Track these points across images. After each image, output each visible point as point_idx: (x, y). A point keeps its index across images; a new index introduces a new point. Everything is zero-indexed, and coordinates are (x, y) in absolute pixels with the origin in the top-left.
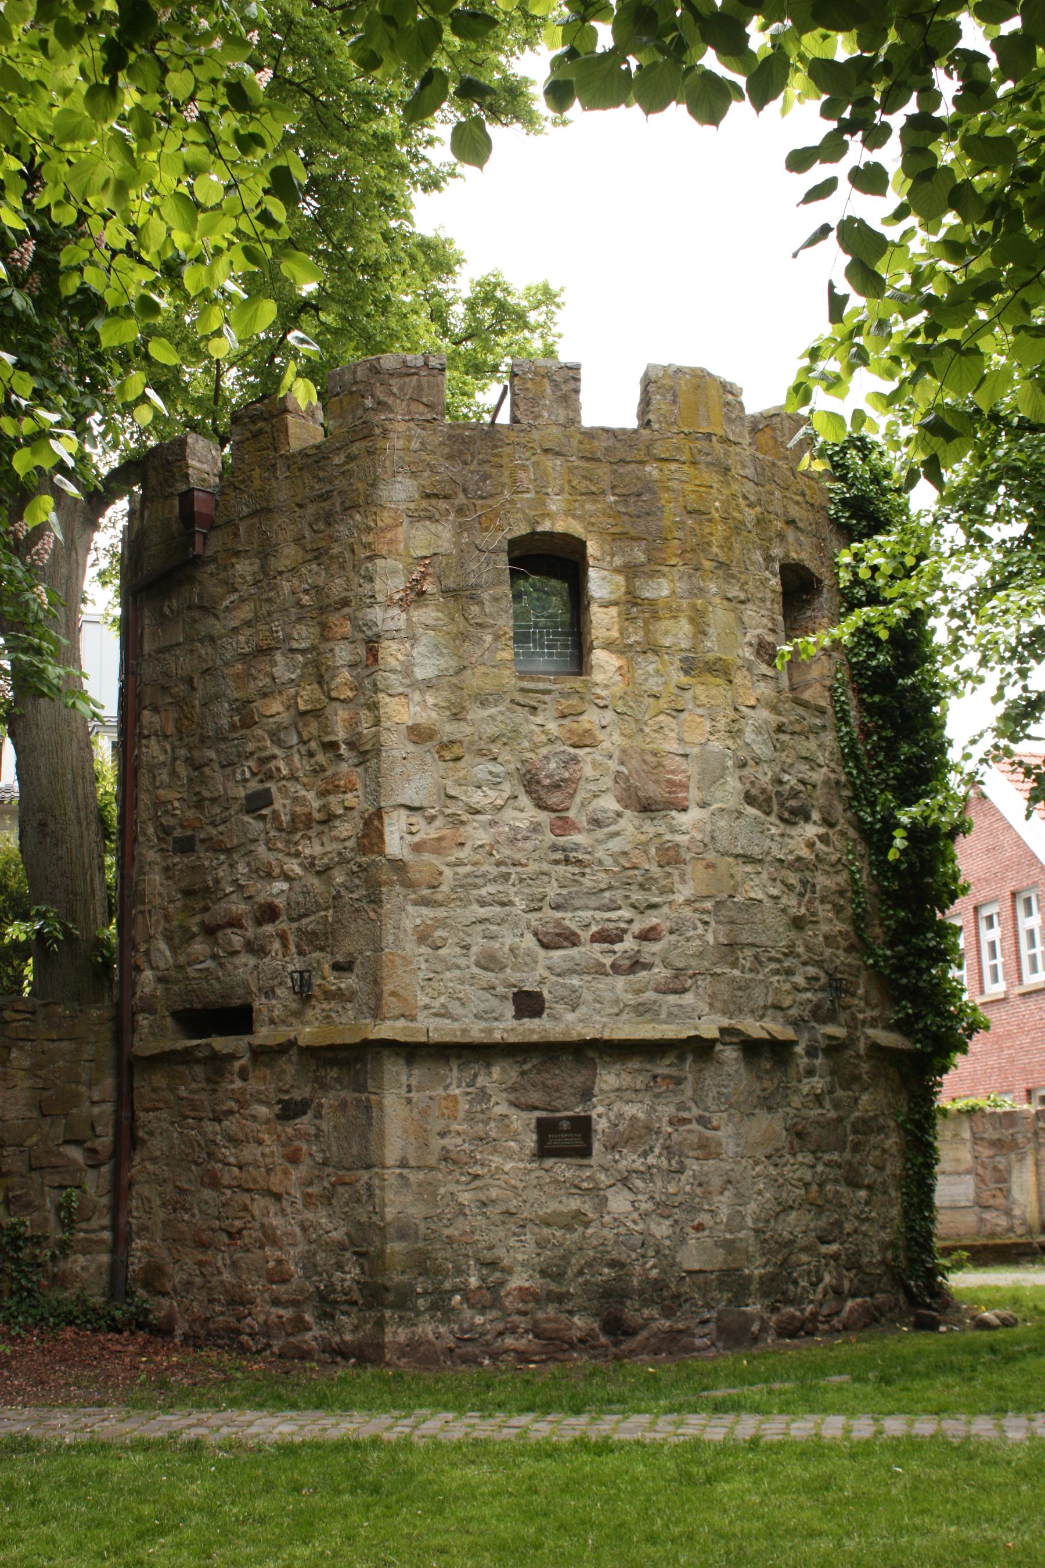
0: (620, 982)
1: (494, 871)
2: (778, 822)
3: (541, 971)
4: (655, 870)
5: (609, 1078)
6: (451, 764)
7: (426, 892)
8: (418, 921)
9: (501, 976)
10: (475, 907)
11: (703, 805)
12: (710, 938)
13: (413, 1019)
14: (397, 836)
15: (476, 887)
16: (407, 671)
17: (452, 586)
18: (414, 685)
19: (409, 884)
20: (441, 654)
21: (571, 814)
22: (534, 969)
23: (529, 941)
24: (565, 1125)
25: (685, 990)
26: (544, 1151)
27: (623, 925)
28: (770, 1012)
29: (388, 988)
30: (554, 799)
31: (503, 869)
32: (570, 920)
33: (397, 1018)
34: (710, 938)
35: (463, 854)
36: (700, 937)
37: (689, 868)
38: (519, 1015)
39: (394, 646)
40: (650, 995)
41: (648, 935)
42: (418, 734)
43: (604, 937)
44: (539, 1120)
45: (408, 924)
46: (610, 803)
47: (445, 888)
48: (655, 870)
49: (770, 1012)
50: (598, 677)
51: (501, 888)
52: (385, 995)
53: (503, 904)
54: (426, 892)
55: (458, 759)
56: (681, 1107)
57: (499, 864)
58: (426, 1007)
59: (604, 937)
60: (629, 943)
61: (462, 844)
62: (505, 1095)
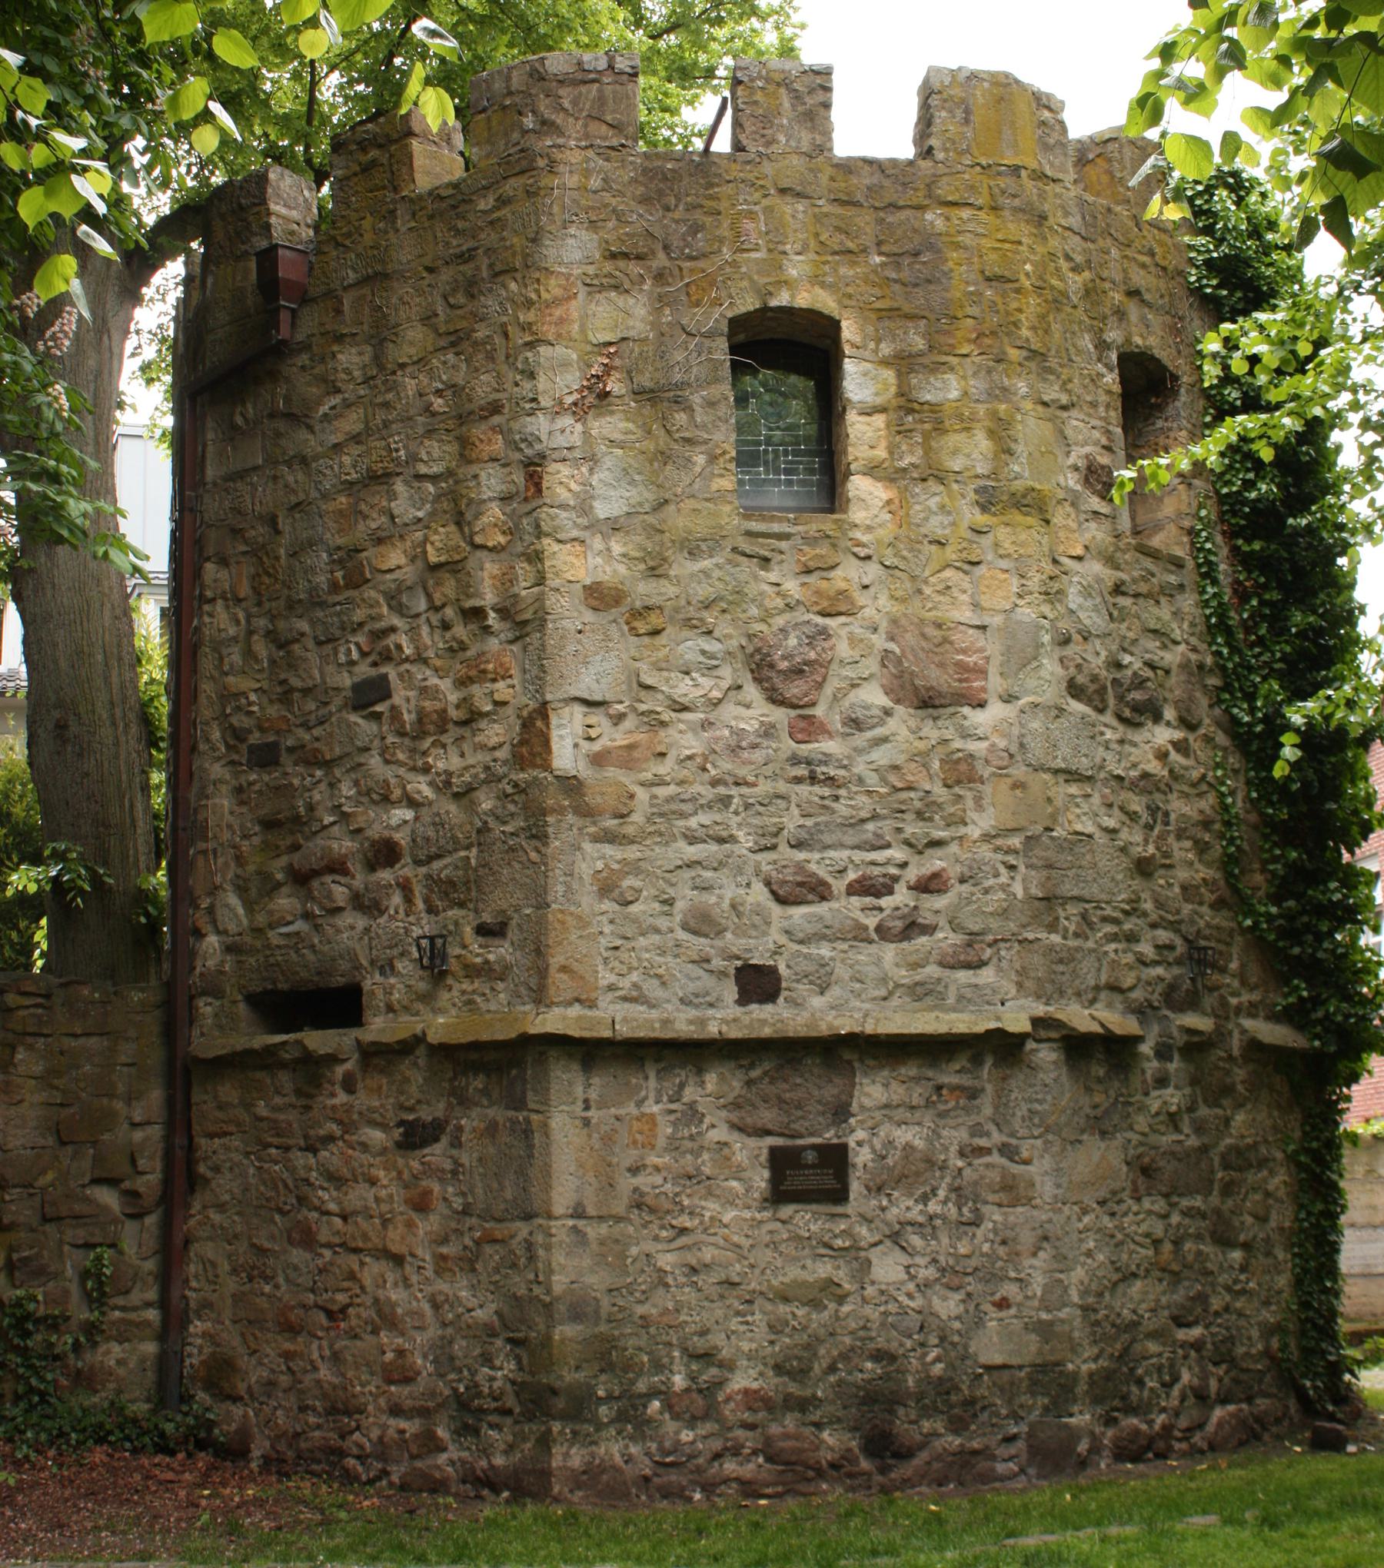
0: (889, 952)
1: (708, 793)
2: (1115, 723)
3: (776, 936)
4: (939, 792)
5: (873, 1090)
6: (646, 640)
7: (611, 823)
8: (600, 865)
9: (718, 943)
10: (681, 844)
11: (1008, 698)
12: (1018, 889)
13: (592, 1004)
15: (683, 815)
16: (584, 507)
17: (648, 384)
18: (593, 526)
19: (587, 812)
20: (632, 482)
21: (819, 711)
22: (765, 934)
23: (759, 894)
24: (810, 1157)
25: (982, 964)
26: (779, 1195)
27: (893, 871)
29: (556, 960)
30: (794, 689)
31: (722, 790)
32: (818, 864)
34: (1018, 889)
35: (664, 768)
36: (1004, 888)
37: (987, 789)
38: (744, 999)
39: (565, 470)
40: (932, 970)
41: (929, 885)
42: (599, 597)
43: (869, 888)
44: (773, 1150)
45: (585, 869)
46: (874, 696)
47: (637, 818)
48: (939, 792)
49: (1103, 995)
50: (857, 515)
51: (718, 818)
52: (552, 970)
53: (721, 841)
54: (611, 823)
55: (656, 632)
56: (977, 1131)
57: (715, 783)
58: (611, 988)
59: (869, 888)
60: (901, 897)
61: (663, 755)
62: (724, 1114)
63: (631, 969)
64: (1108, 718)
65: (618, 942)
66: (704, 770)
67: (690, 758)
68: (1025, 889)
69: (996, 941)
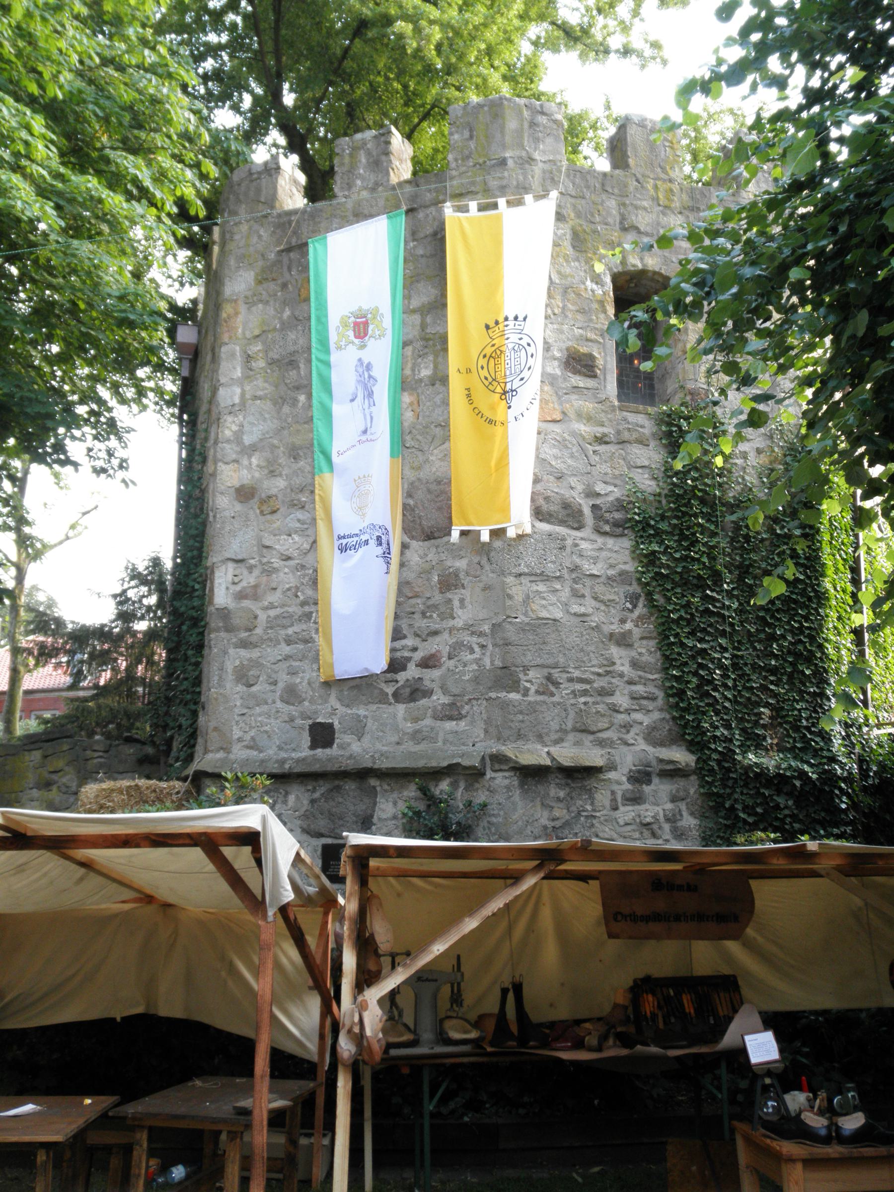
2: (595, 537)
4: (438, 598)
6: (269, 517)
7: (244, 635)
8: (237, 663)
9: (300, 708)
12: (487, 662)
13: (227, 750)
14: (224, 586)
15: (285, 627)
17: (276, 357)
19: (229, 629)
20: (265, 420)
22: (326, 701)
25: (460, 717)
27: (406, 654)
28: (571, 737)
31: (307, 609)
33: (218, 750)
34: (487, 662)
35: (274, 598)
36: (477, 661)
37: (466, 593)
39: (230, 419)
40: (428, 721)
41: (427, 663)
42: (245, 494)
45: (229, 666)
47: (259, 631)
48: (438, 598)
49: (571, 737)
51: (304, 627)
52: (210, 731)
53: (306, 641)
54: (244, 635)
55: (274, 512)
57: (303, 604)
58: (240, 740)
60: (412, 672)
62: (299, 822)
63: (251, 728)
64: (587, 532)
65: (245, 711)
66: (297, 596)
67: (289, 589)
68: (492, 662)
69: (470, 700)
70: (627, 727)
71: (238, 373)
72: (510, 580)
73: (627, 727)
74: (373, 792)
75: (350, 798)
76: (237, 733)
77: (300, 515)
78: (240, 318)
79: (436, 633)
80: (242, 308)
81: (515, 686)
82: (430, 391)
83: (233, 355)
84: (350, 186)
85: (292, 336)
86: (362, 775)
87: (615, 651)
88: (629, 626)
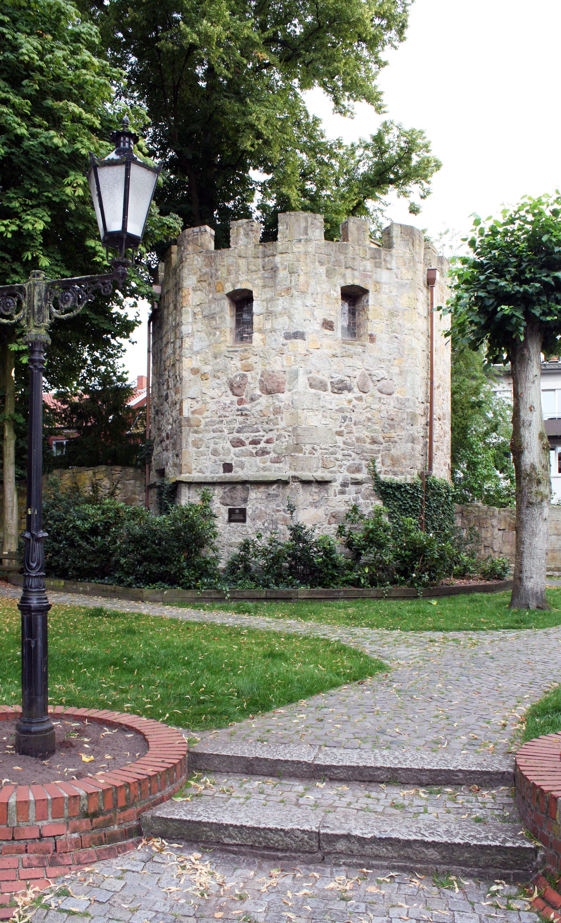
0: (258, 459)
1: (218, 419)
3: (232, 455)
4: (272, 417)
5: (254, 494)
11: (289, 391)
16: (191, 348)
18: (193, 353)
19: (190, 426)
21: (244, 397)
23: (229, 445)
24: (237, 511)
26: (230, 520)
30: (237, 391)
32: (242, 436)
37: (284, 415)
38: (225, 472)
39: (187, 339)
40: (269, 464)
42: (195, 371)
43: (255, 442)
44: (230, 509)
46: (258, 392)
47: (202, 427)
48: (272, 417)
50: (254, 343)
56: (278, 505)
59: (255, 442)
60: (262, 445)
70: (341, 466)
71: (190, 320)
72: (300, 411)
73: (341, 466)
74: (248, 490)
75: (239, 492)
76: (194, 466)
77: (218, 381)
78: (190, 296)
79: (271, 430)
80: (191, 292)
81: (301, 451)
82: (270, 334)
83: (188, 312)
84: (237, 244)
85: (213, 306)
86: (244, 483)
87: (338, 438)
88: (343, 428)
